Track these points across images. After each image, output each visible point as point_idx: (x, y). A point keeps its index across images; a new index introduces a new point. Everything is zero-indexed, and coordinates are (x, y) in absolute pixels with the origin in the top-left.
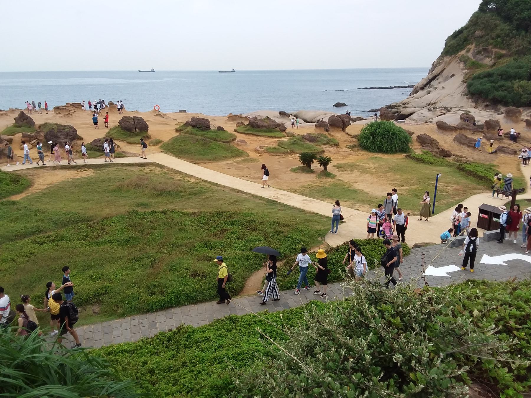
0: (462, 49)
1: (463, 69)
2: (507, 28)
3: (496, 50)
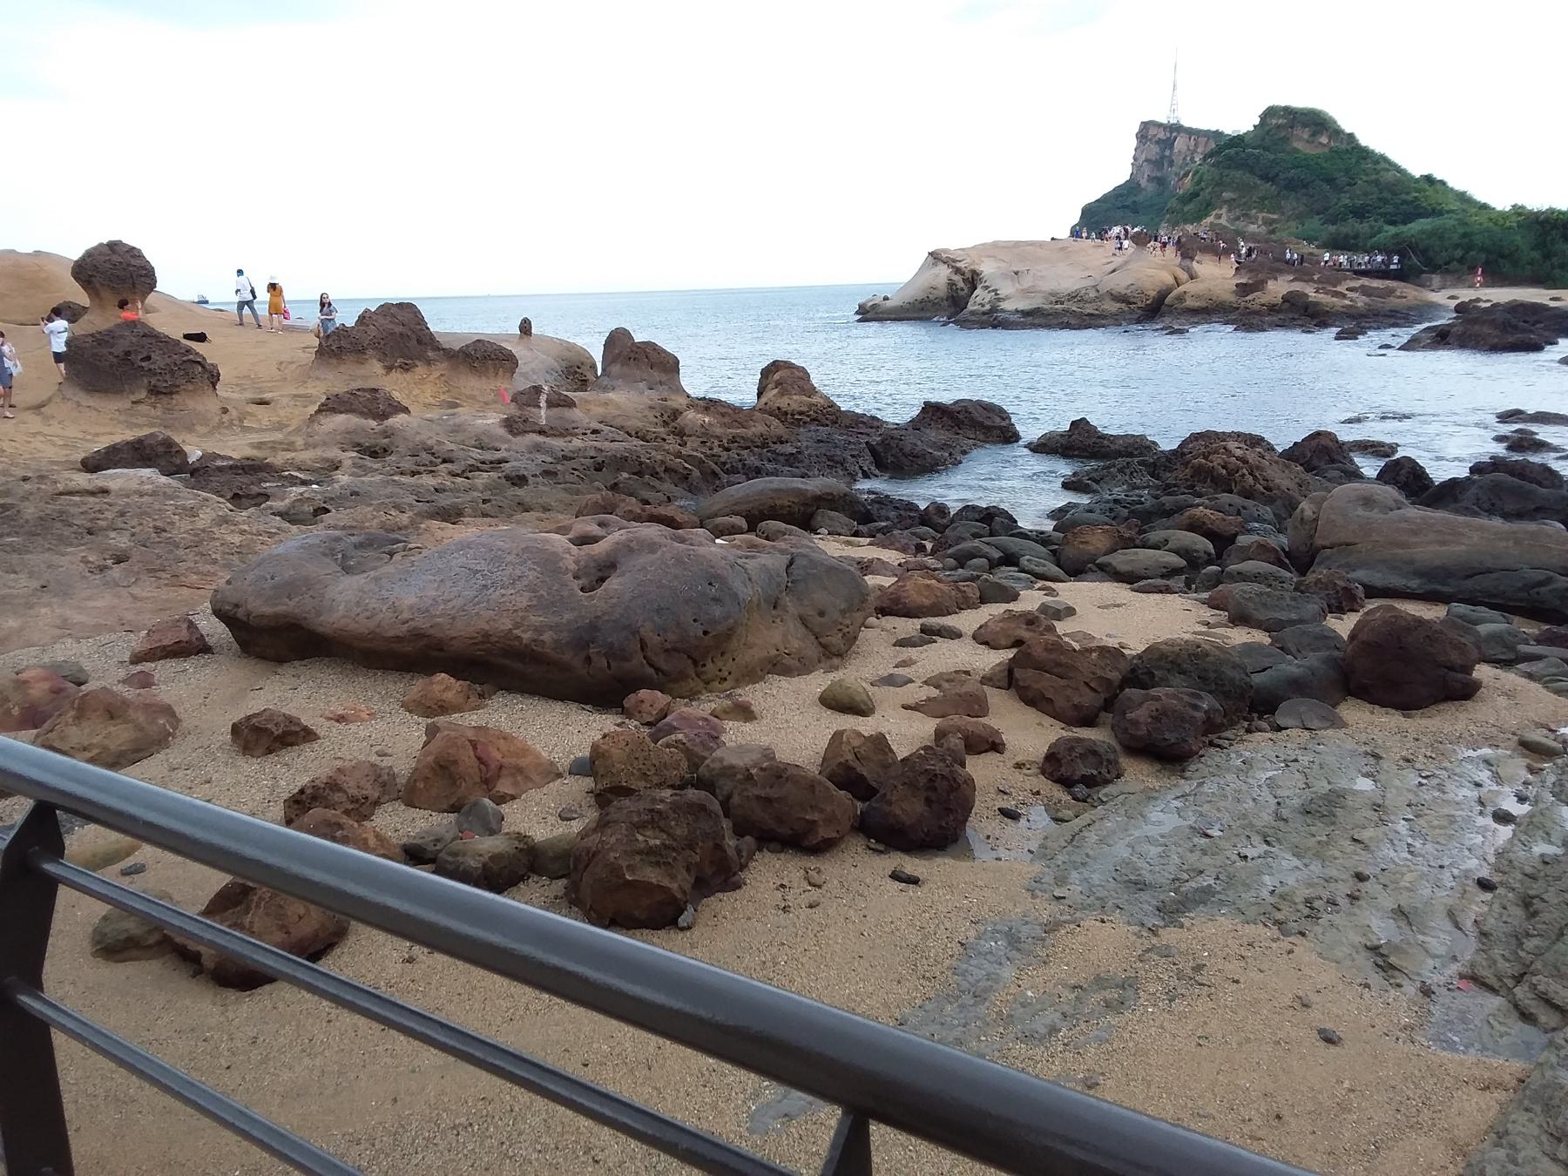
0: (1207, 215)
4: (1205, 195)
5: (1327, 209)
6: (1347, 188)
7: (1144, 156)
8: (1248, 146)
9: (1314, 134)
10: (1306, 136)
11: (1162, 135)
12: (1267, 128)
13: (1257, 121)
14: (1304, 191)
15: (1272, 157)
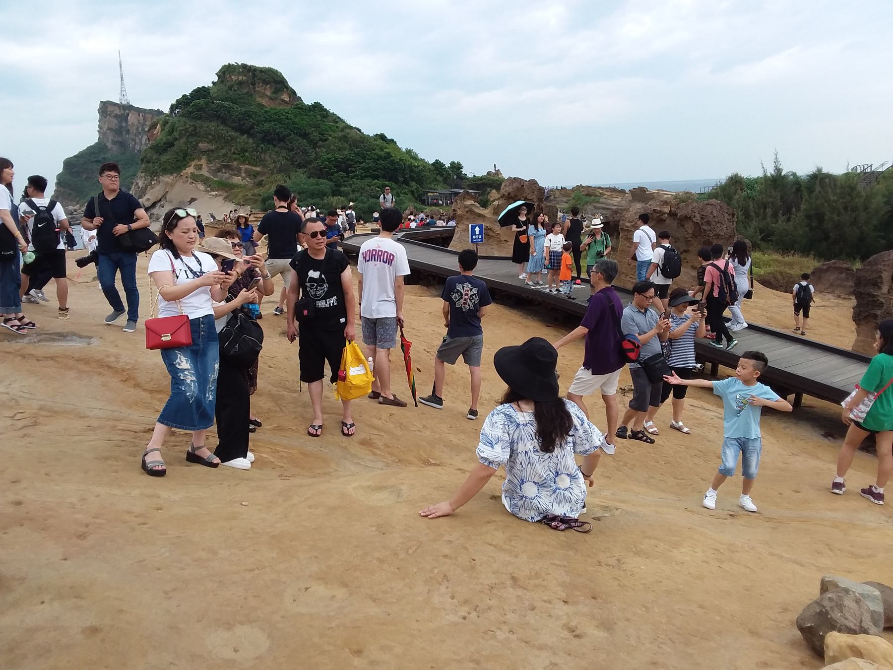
0: (186, 166)
1: (208, 191)
2: (251, 140)
3: (246, 166)
4: (181, 144)
5: (310, 162)
6: (320, 143)
7: (106, 126)
8: (214, 98)
9: (276, 91)
10: (268, 93)
11: (117, 111)
12: (228, 84)
13: (216, 79)
14: (282, 144)
15: (244, 109)
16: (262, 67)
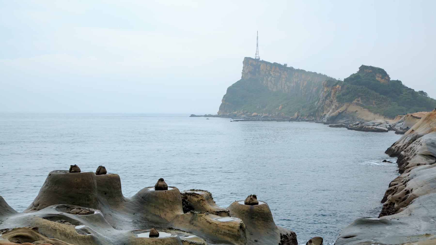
16: (377, 67)
